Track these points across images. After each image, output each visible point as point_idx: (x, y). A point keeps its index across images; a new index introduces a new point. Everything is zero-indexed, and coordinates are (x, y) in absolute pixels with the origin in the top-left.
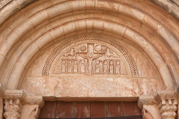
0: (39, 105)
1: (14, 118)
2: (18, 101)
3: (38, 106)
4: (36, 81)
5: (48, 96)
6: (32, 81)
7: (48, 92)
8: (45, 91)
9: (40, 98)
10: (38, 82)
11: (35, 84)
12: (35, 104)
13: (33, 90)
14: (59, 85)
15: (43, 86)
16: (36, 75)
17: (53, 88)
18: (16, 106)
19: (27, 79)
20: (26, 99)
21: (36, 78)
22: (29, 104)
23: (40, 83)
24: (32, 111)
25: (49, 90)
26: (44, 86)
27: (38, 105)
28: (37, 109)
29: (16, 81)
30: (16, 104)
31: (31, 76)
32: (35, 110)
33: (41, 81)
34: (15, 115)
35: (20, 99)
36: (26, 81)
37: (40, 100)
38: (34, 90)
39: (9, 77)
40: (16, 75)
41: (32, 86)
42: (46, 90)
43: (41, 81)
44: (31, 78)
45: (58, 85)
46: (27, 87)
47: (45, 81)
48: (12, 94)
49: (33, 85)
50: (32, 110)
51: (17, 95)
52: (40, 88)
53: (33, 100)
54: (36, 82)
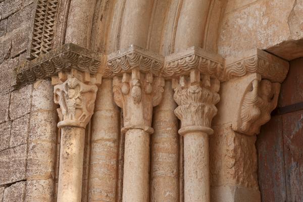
0: (257, 72)
1: (192, 117)
2: (193, 76)
3: (255, 77)
4: (246, 16)
5: (275, 44)
6: (239, 19)
7: (274, 33)
8: (268, 35)
9: (253, 54)
10: (251, 18)
11: (245, 25)
12: (247, 73)
13: (243, 41)
14: (299, 6)
15: (261, 23)
16: (244, 4)
17: (284, 19)
18: (192, 87)
19: (228, 20)
20: (226, 66)
21: (245, 10)
22: (234, 76)
23: (255, 18)
24: (245, 94)
25: (276, 30)
26: (265, 22)
27: (255, 74)
28: (255, 85)
29: (189, 30)
30: (192, 84)
31: (234, 10)
32: (250, 88)
33: (257, 13)
34: (193, 109)
35: (195, 67)
36: (228, 26)
37: (253, 59)
38: (245, 39)
39: (176, 26)
40: (186, 18)
41: (239, 32)
42: (270, 32)
43: (257, 13)
44: (236, 14)
45: (295, 9)
46: (231, 37)
47: (264, 9)
48: (176, 62)
49: (241, 31)
50: (244, 91)
51: (185, 62)
52: (256, 31)
53: (240, 63)
54: (248, 19)
